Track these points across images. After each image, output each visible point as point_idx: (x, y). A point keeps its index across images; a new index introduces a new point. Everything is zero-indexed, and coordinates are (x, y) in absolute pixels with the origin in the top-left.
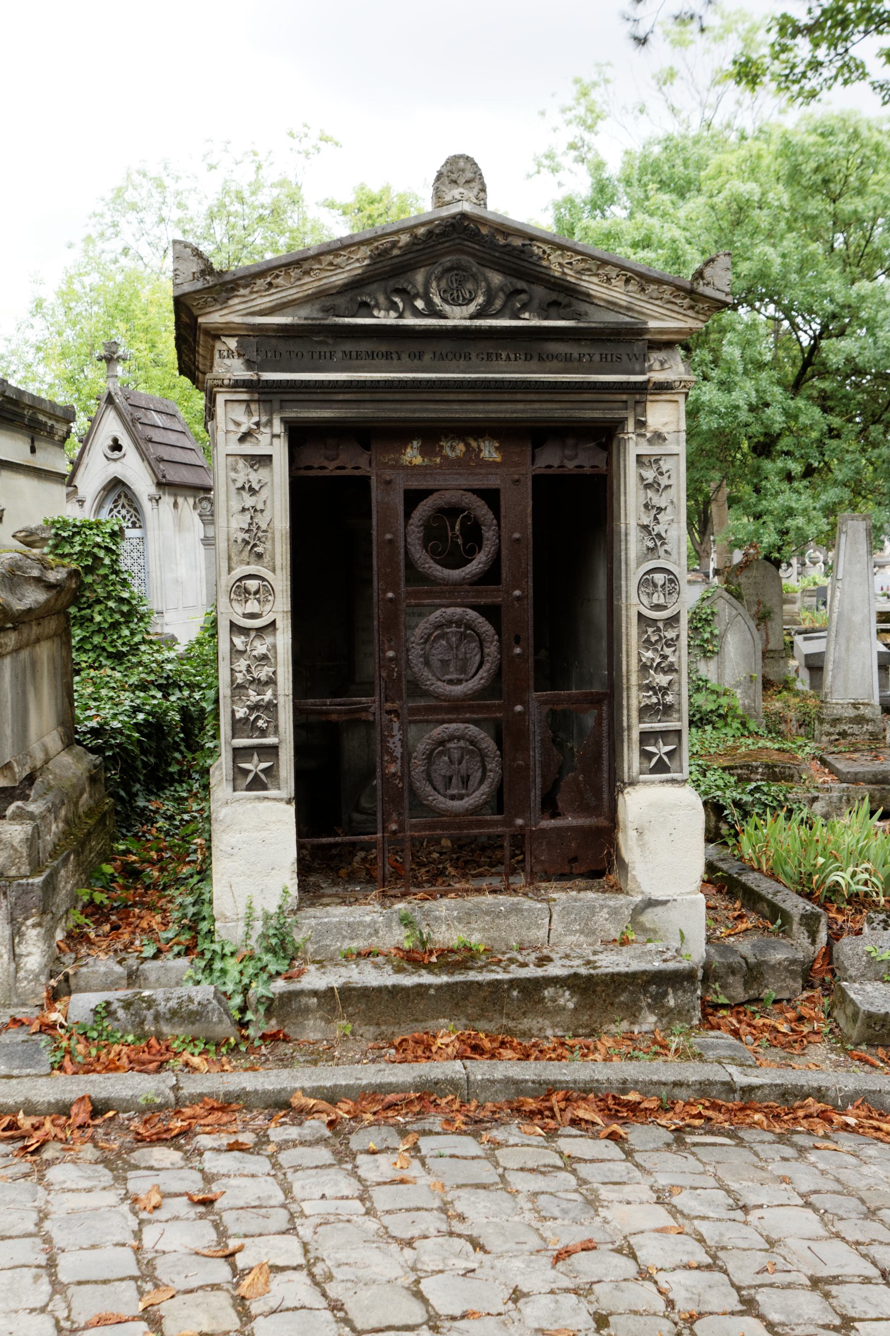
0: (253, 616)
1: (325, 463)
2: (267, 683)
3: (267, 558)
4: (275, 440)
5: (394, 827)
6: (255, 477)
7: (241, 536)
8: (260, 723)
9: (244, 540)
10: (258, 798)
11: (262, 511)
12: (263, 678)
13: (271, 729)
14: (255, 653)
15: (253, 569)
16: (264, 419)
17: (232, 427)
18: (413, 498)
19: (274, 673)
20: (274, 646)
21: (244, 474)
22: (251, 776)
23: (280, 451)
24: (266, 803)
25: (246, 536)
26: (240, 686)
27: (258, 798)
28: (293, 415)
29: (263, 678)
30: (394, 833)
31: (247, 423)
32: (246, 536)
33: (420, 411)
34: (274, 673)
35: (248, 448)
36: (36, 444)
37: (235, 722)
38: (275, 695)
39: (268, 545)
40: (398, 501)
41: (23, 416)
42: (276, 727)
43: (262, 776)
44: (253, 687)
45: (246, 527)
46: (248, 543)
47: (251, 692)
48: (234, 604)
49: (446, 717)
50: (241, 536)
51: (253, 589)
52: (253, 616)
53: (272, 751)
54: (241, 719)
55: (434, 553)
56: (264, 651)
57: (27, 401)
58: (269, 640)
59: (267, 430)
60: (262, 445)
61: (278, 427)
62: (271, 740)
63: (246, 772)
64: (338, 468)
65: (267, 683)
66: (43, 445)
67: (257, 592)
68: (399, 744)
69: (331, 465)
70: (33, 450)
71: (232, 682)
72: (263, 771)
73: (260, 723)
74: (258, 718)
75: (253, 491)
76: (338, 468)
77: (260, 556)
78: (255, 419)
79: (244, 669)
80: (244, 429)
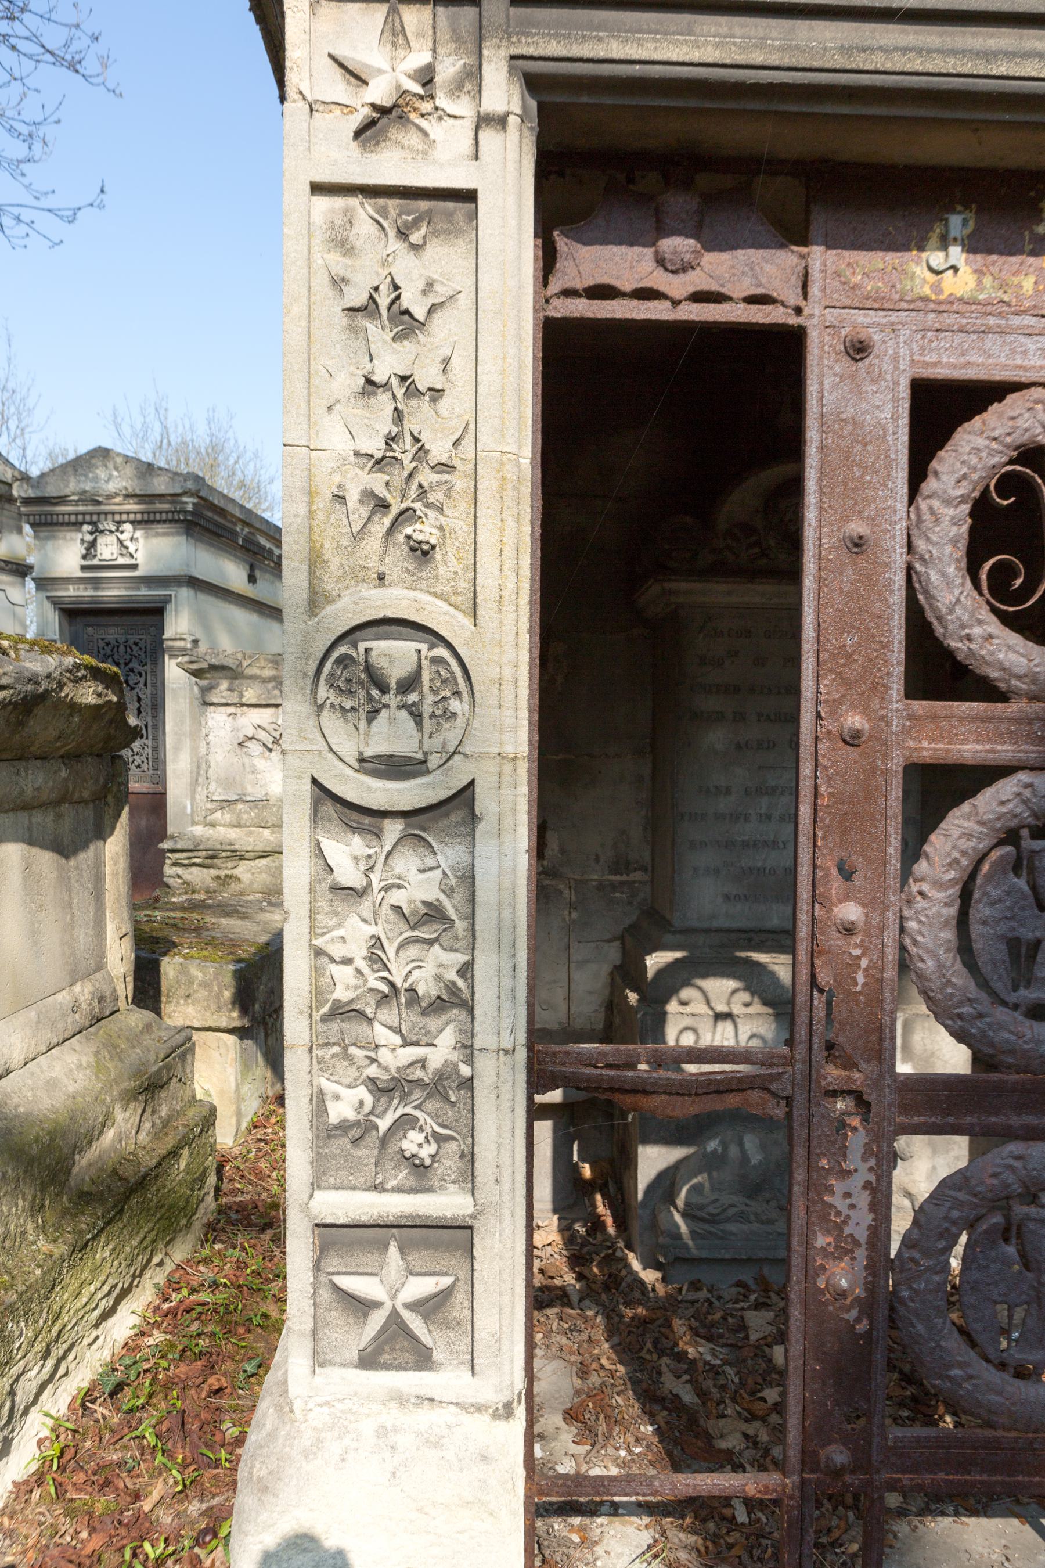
0: (394, 767)
1: (660, 280)
2: (438, 1006)
3: (448, 564)
4: (489, 137)
5: (838, 1455)
6: (420, 270)
7: (360, 481)
8: (412, 1142)
9: (368, 495)
10: (400, 1399)
11: (436, 393)
12: (427, 988)
13: (450, 1163)
14: (397, 897)
15: (398, 600)
16: (449, 68)
17: (338, 89)
18: (940, 409)
19: (466, 970)
20: (469, 878)
21: (376, 256)
22: (377, 1320)
23: (505, 177)
24: (426, 1418)
25: (377, 482)
26: (341, 1012)
27: (400, 1399)
28: (554, 48)
29: (427, 988)
30: (837, 1473)
31: (389, 76)
32: (377, 482)
33: (1010, 55)
34: (466, 970)
35: (389, 166)
36: (257, 573)
37: (327, 1133)
38: (468, 1049)
39: (457, 517)
40: (891, 418)
41: (235, 534)
42: (469, 1157)
43: (415, 1323)
44: (389, 1015)
45: (375, 446)
46: (383, 506)
47: (382, 1034)
48: (330, 721)
49: (1016, 1121)
50: (360, 481)
51: (395, 673)
52: (394, 767)
53: (456, 1236)
54: (343, 1127)
55: (1000, 590)
56: (433, 894)
57: (237, 513)
58: (449, 855)
59: (463, 107)
60: (438, 152)
61: (501, 92)
62: (447, 1203)
63: (360, 1307)
64: (700, 297)
65: (438, 1006)
66: (267, 576)
67: (410, 683)
68: (863, 1200)
69: (678, 286)
70: (252, 579)
71: (318, 994)
72: (414, 1306)
73: (412, 1142)
74: (405, 1123)
75: (406, 324)
76: (700, 297)
77: (422, 553)
78: (420, 58)
79: (359, 952)
80: (379, 92)
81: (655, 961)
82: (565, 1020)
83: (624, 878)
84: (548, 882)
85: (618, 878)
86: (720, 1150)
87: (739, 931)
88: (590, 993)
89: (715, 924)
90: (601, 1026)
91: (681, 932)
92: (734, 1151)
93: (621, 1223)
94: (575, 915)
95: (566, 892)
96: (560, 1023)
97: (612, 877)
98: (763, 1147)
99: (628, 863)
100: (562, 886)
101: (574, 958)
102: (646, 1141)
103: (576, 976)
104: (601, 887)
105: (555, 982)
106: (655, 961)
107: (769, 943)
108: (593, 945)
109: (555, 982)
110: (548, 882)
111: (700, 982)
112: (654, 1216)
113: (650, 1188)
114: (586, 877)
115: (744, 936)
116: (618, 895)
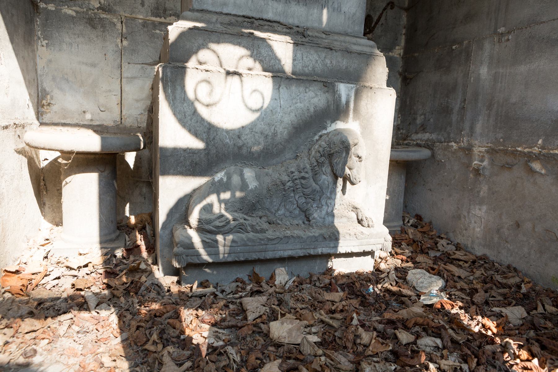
81: (175, 30)
82: (118, 119)
83: (162, 20)
84: (104, 16)
85: (158, 19)
86: (225, 179)
87: (244, 16)
88: (137, 101)
89: (225, 11)
90: (145, 125)
91: (198, 11)
92: (236, 179)
93: (151, 249)
94: (125, 43)
95: (119, 25)
96: (115, 121)
97: (154, 19)
98: (258, 177)
99: (165, 10)
100: (115, 20)
101: (125, 75)
102: (165, 173)
103: (126, 88)
104: (145, 24)
105: (110, 91)
106: (175, 30)
107: (266, 27)
108: (139, 66)
109: (110, 91)
110: (104, 16)
111: (213, 46)
112: (172, 234)
113: (171, 213)
114: (134, 16)
115: (246, 20)
116: (158, 31)
